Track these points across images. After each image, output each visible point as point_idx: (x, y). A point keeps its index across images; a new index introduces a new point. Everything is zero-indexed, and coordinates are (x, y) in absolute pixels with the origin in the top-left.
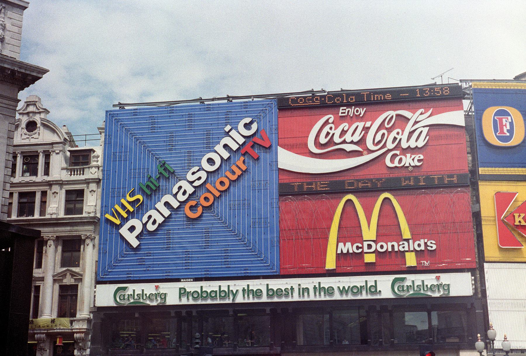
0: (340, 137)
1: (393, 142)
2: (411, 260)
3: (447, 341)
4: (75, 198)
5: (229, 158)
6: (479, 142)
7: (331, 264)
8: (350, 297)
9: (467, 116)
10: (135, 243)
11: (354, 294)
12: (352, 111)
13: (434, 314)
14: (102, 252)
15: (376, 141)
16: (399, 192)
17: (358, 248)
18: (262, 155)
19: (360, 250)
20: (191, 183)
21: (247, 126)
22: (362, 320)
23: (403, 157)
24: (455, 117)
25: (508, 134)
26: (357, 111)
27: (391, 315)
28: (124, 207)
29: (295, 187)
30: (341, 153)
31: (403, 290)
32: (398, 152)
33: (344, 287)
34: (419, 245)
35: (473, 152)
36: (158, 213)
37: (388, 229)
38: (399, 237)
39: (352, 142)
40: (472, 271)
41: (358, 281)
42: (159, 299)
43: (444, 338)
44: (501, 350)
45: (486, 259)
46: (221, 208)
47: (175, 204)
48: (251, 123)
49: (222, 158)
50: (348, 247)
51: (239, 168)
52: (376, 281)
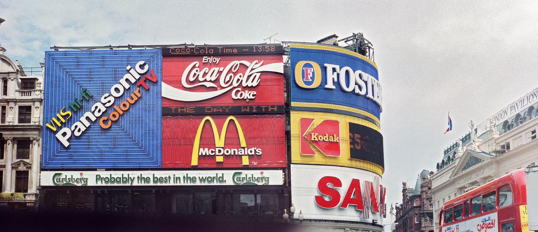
0: (203, 77)
1: (237, 82)
2: (245, 161)
3: (266, 213)
4: (25, 112)
5: (129, 88)
6: (292, 84)
7: (194, 162)
8: (206, 184)
9: (285, 67)
10: (66, 144)
11: (209, 182)
12: (211, 59)
13: (259, 196)
14: (44, 150)
15: (226, 81)
16: (240, 116)
17: (212, 152)
18: (151, 87)
19: (214, 154)
20: (104, 104)
21: (142, 67)
22: (214, 198)
23: (243, 92)
24: (278, 67)
25: (311, 80)
26: (215, 60)
27: (232, 196)
28: (58, 119)
29: (172, 111)
31: (240, 180)
32: (240, 89)
33: (203, 178)
34: (251, 151)
35: (288, 91)
36: (82, 124)
37: (232, 140)
38: (238, 145)
39: (210, 81)
40: (284, 169)
41: (212, 174)
42: (83, 182)
43: (264, 212)
44: (298, 219)
45: (292, 162)
46: (124, 122)
47: (93, 119)
48: (144, 64)
49: (124, 88)
50: (206, 151)
51: (136, 96)
52: (223, 174)
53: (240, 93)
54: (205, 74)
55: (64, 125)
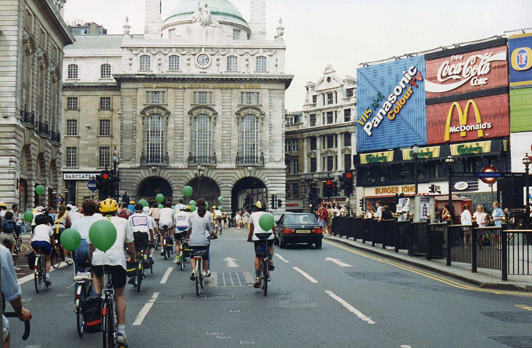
4: (347, 112)
12: (457, 57)
14: (358, 137)
20: (390, 102)
25: (524, 63)
29: (433, 101)
30: (451, 81)
32: (476, 78)
36: (378, 118)
37: (470, 119)
39: (456, 74)
47: (384, 113)
50: (454, 129)
53: (476, 81)
54: (453, 69)
55: (368, 120)
